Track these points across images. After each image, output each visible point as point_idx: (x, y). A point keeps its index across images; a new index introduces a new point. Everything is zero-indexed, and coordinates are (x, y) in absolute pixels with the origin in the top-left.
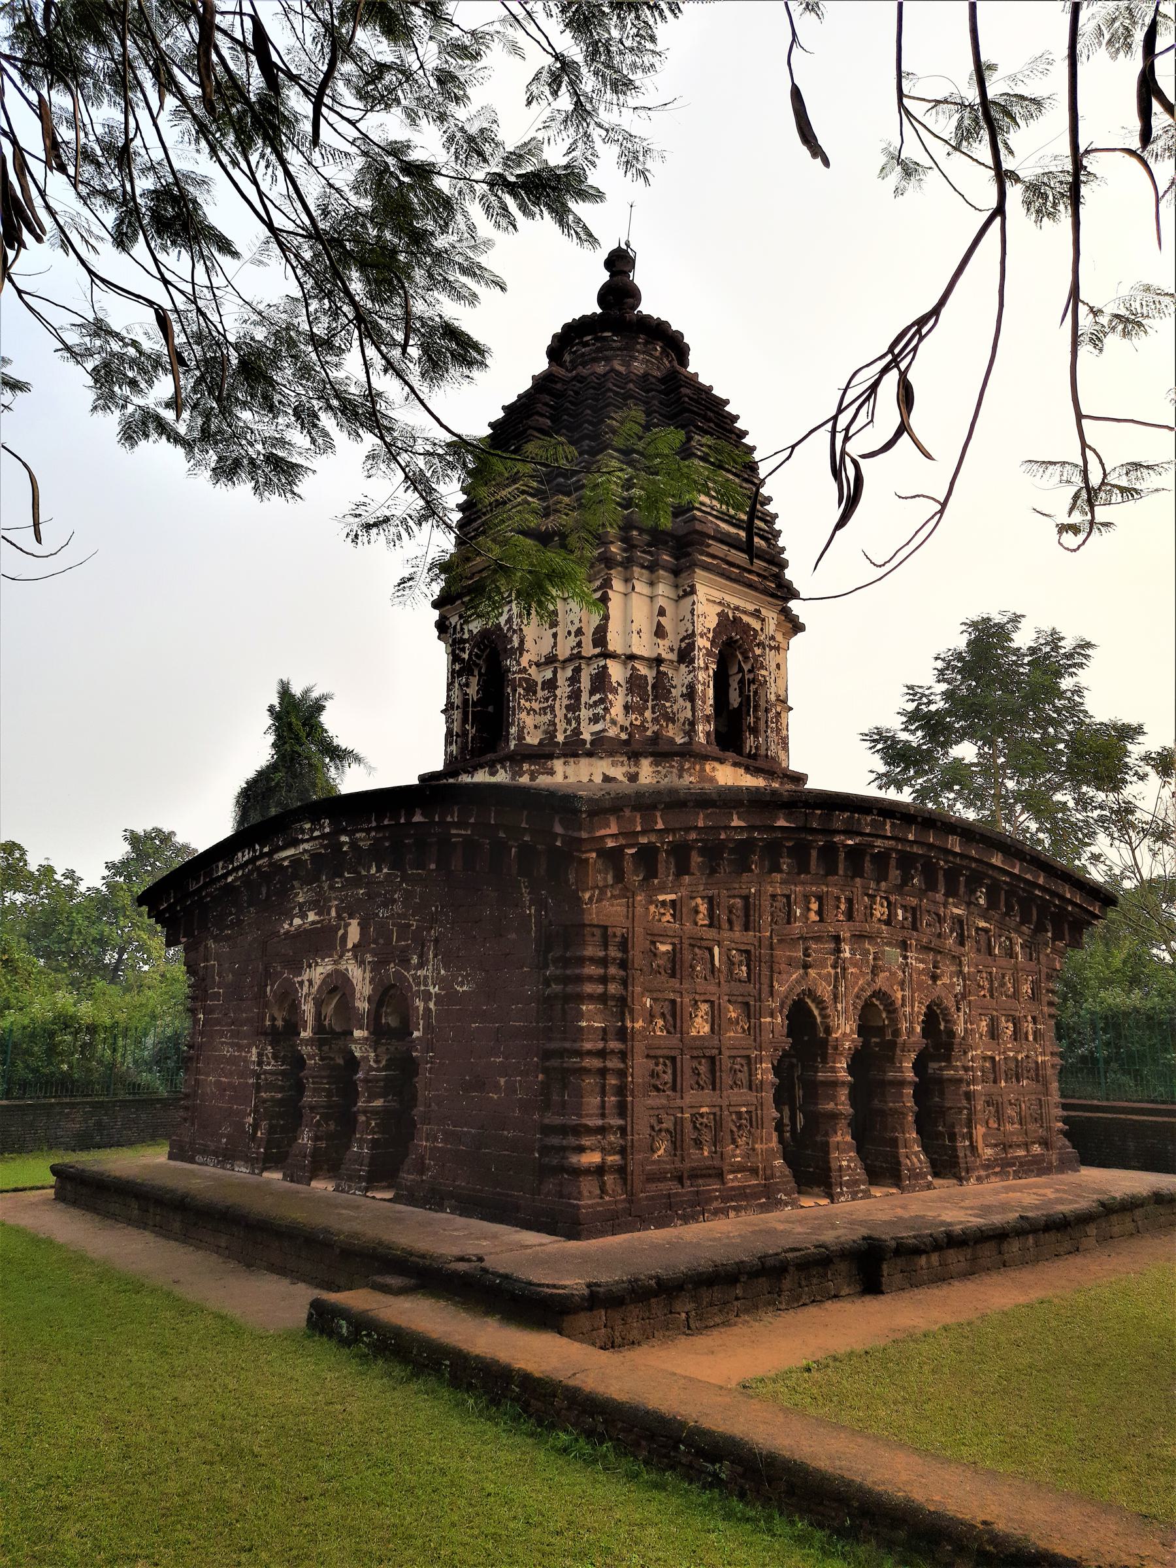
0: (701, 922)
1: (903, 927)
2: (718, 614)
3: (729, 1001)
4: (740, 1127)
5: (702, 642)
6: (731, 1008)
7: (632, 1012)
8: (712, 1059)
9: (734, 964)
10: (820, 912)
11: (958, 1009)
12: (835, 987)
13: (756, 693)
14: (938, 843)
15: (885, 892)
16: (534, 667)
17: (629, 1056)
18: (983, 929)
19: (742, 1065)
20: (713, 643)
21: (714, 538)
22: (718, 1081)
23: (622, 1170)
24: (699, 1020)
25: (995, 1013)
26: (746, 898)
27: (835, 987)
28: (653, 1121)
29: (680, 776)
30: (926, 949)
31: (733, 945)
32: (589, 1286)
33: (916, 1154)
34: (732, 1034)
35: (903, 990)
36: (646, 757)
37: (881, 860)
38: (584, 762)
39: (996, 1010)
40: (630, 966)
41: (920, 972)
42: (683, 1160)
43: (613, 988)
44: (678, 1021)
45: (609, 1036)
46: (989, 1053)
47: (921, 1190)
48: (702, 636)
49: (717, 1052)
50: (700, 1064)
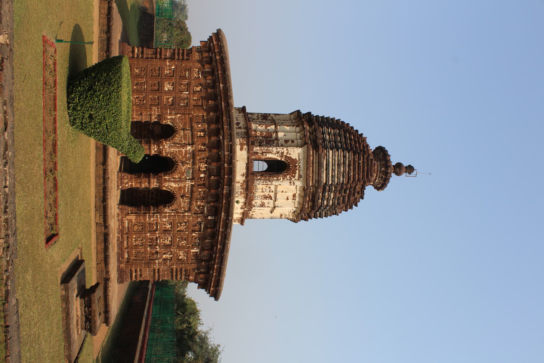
0: (194, 87)
1: (198, 179)
2: (296, 159)
3: (174, 97)
4: (140, 100)
5: (285, 149)
6: (172, 99)
7: (172, 61)
8: (158, 90)
9: (184, 100)
10: (200, 136)
11: (172, 210)
12: (178, 144)
13: (274, 176)
14: (225, 180)
15: (209, 168)
16: (271, 118)
17: (160, 60)
18: (201, 227)
19: (156, 103)
20: (286, 156)
21: (319, 153)
22: (153, 91)
23: (133, 57)
24: (169, 86)
25: (172, 232)
26: (202, 106)
27: (178, 144)
28: (143, 69)
29: (241, 137)
30: (192, 192)
31: (189, 100)
32: (113, 8)
33: (127, 183)
34: (165, 100)
35: (178, 178)
36: (246, 130)
37: (219, 159)
38: (244, 119)
39: (173, 232)
40: (182, 61)
41: (184, 189)
42: (134, 78)
43: (177, 57)
44: (169, 77)
45: (165, 56)
46: (159, 227)
47: (118, 183)
48: (287, 150)
49: (160, 92)
50: (157, 86)
